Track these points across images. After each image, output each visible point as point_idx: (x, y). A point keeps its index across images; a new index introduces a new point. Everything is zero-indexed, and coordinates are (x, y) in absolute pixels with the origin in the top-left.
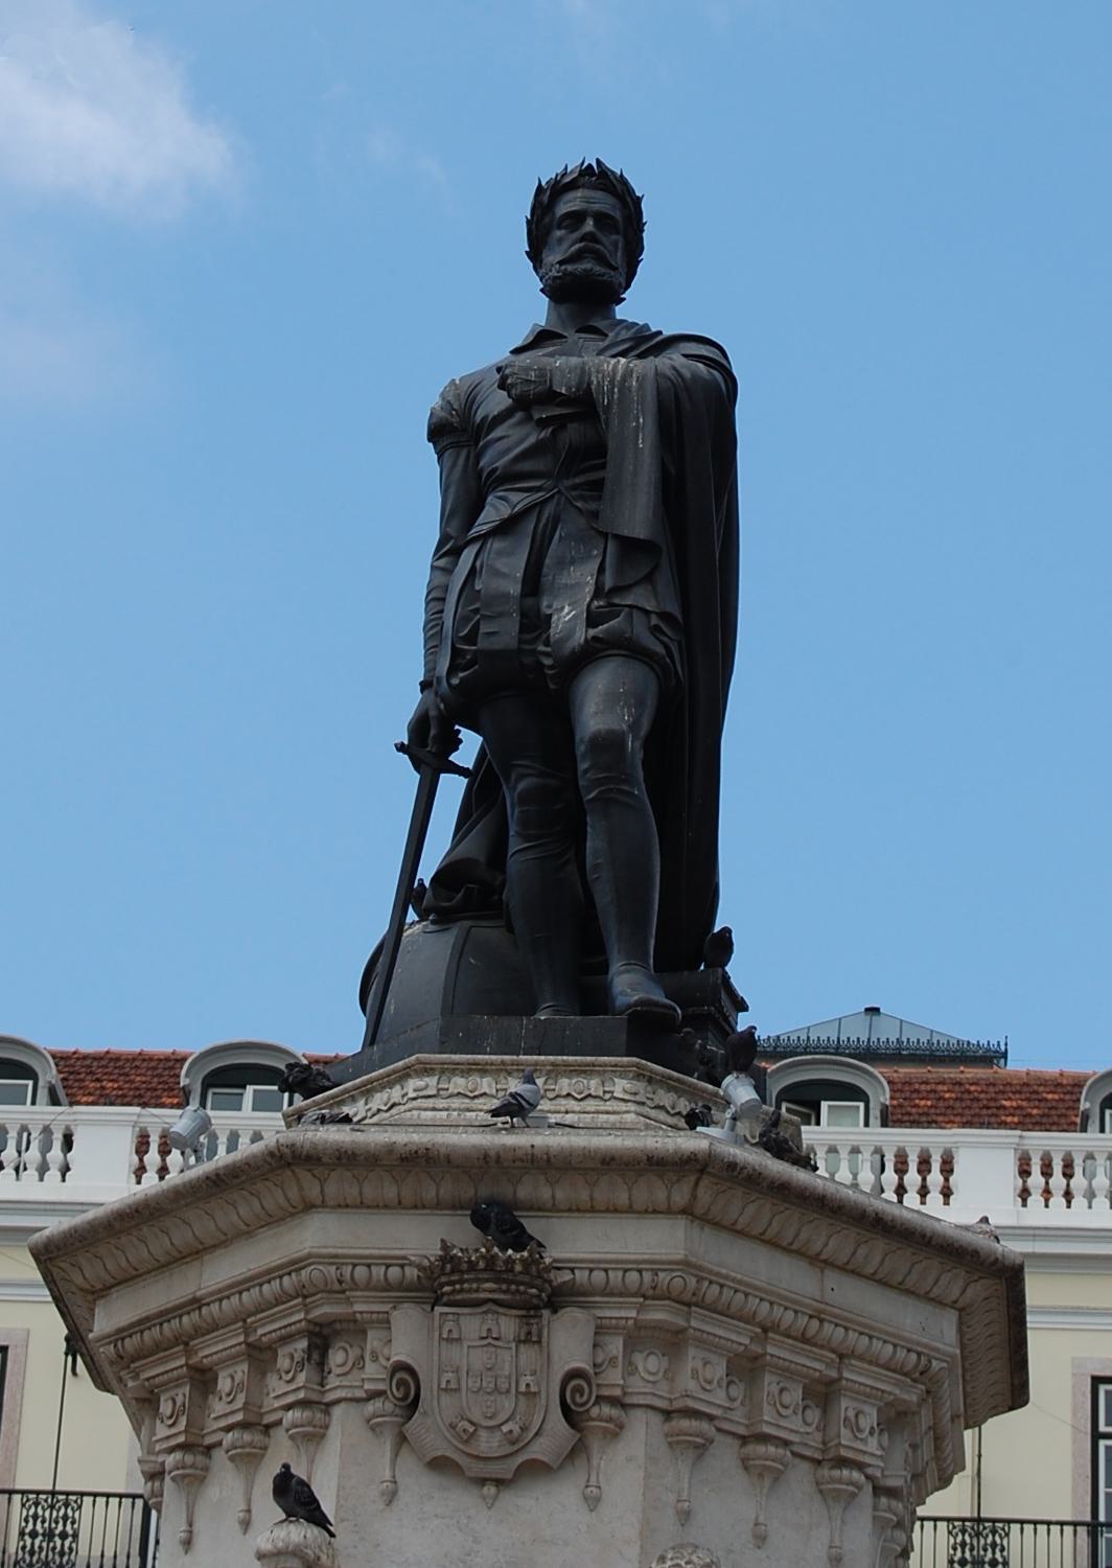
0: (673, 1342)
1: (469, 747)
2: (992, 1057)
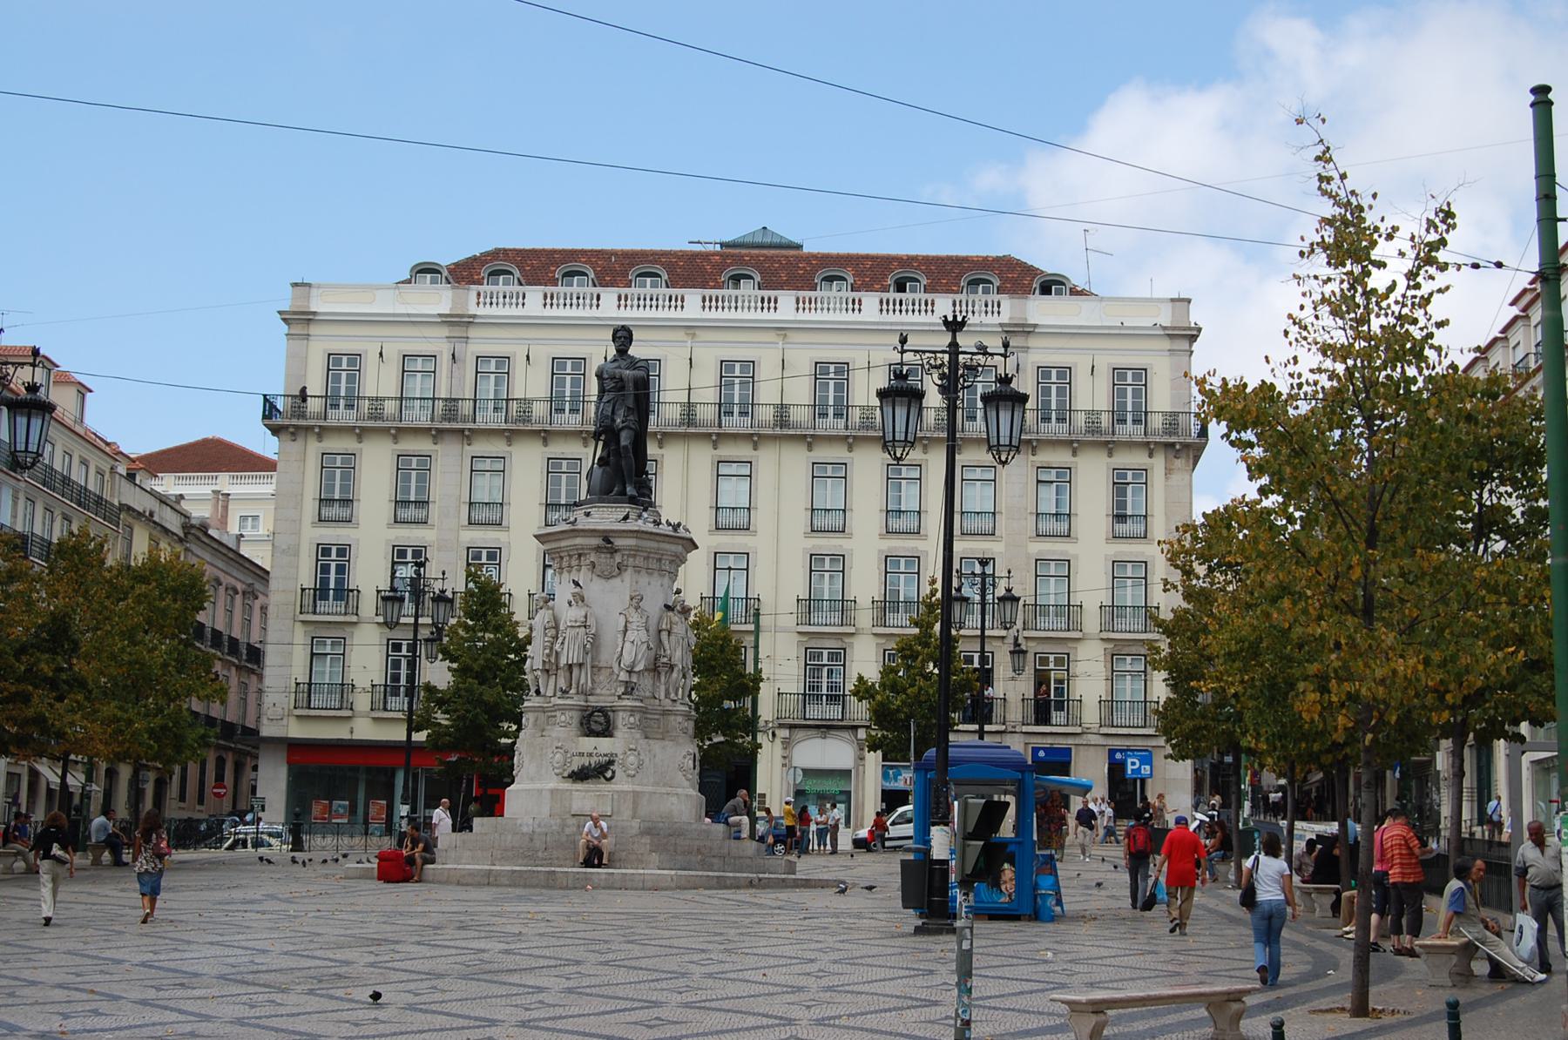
0: (634, 556)
2: (799, 247)
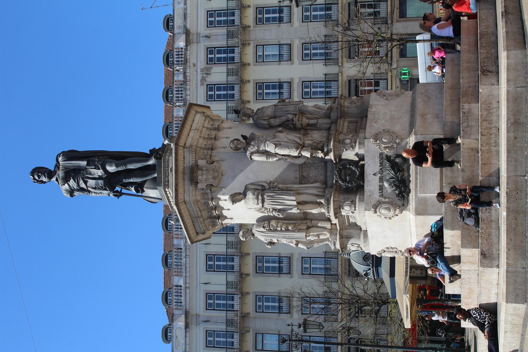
1: (118, 188)
